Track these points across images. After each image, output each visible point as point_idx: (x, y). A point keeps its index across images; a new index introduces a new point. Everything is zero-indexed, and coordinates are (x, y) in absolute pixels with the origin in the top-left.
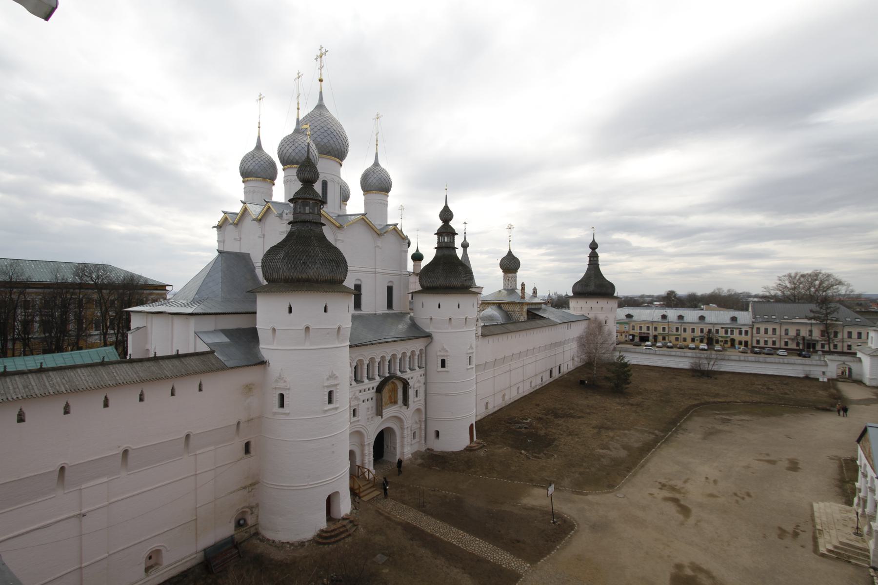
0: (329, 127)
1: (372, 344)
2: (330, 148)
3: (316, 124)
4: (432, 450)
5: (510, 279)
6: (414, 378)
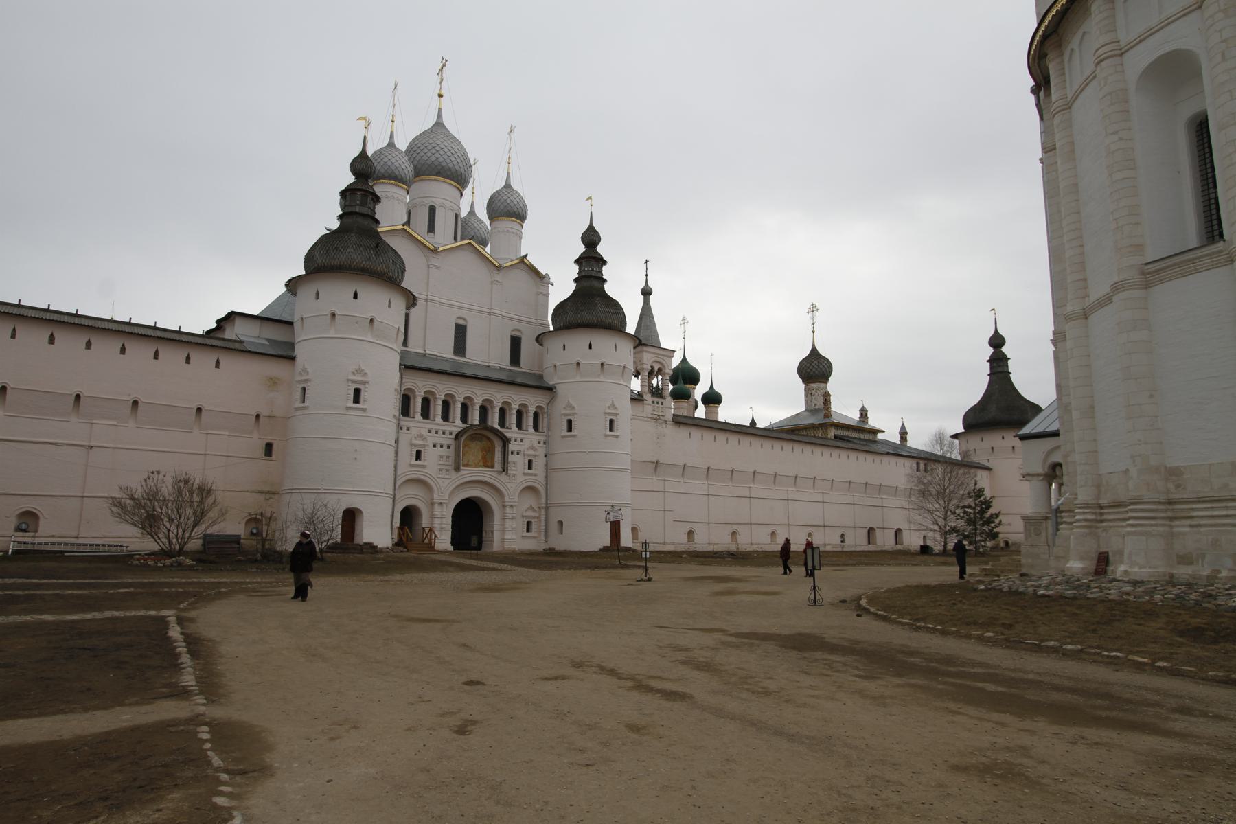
2: (440, 168)
4: (554, 549)
5: (813, 392)
6: (523, 442)
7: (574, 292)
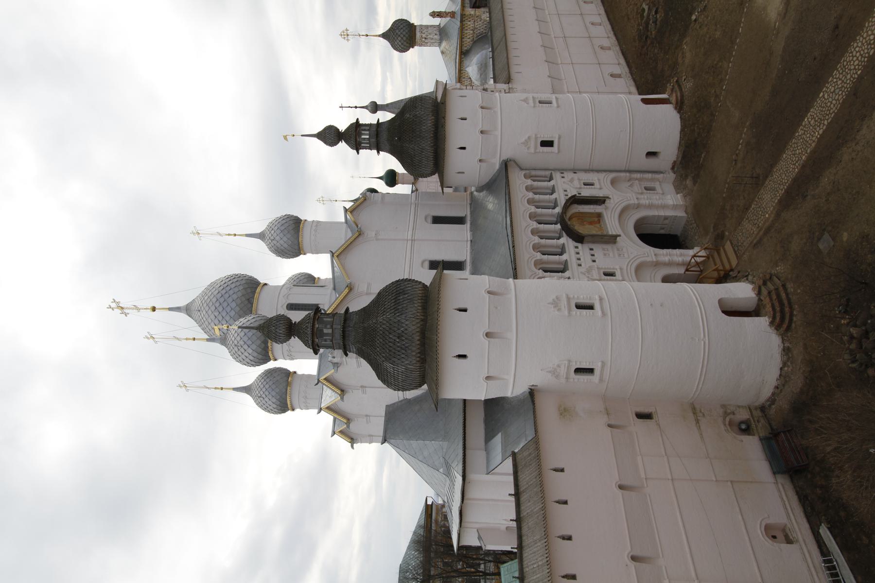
0: (214, 300)
1: (513, 247)
2: (244, 299)
3: (212, 317)
4: (675, 162)
5: (424, 36)
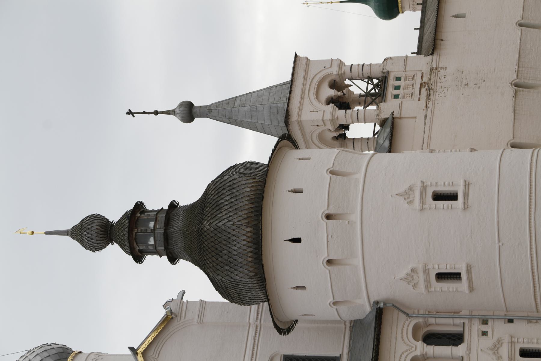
7: (196, 263)
